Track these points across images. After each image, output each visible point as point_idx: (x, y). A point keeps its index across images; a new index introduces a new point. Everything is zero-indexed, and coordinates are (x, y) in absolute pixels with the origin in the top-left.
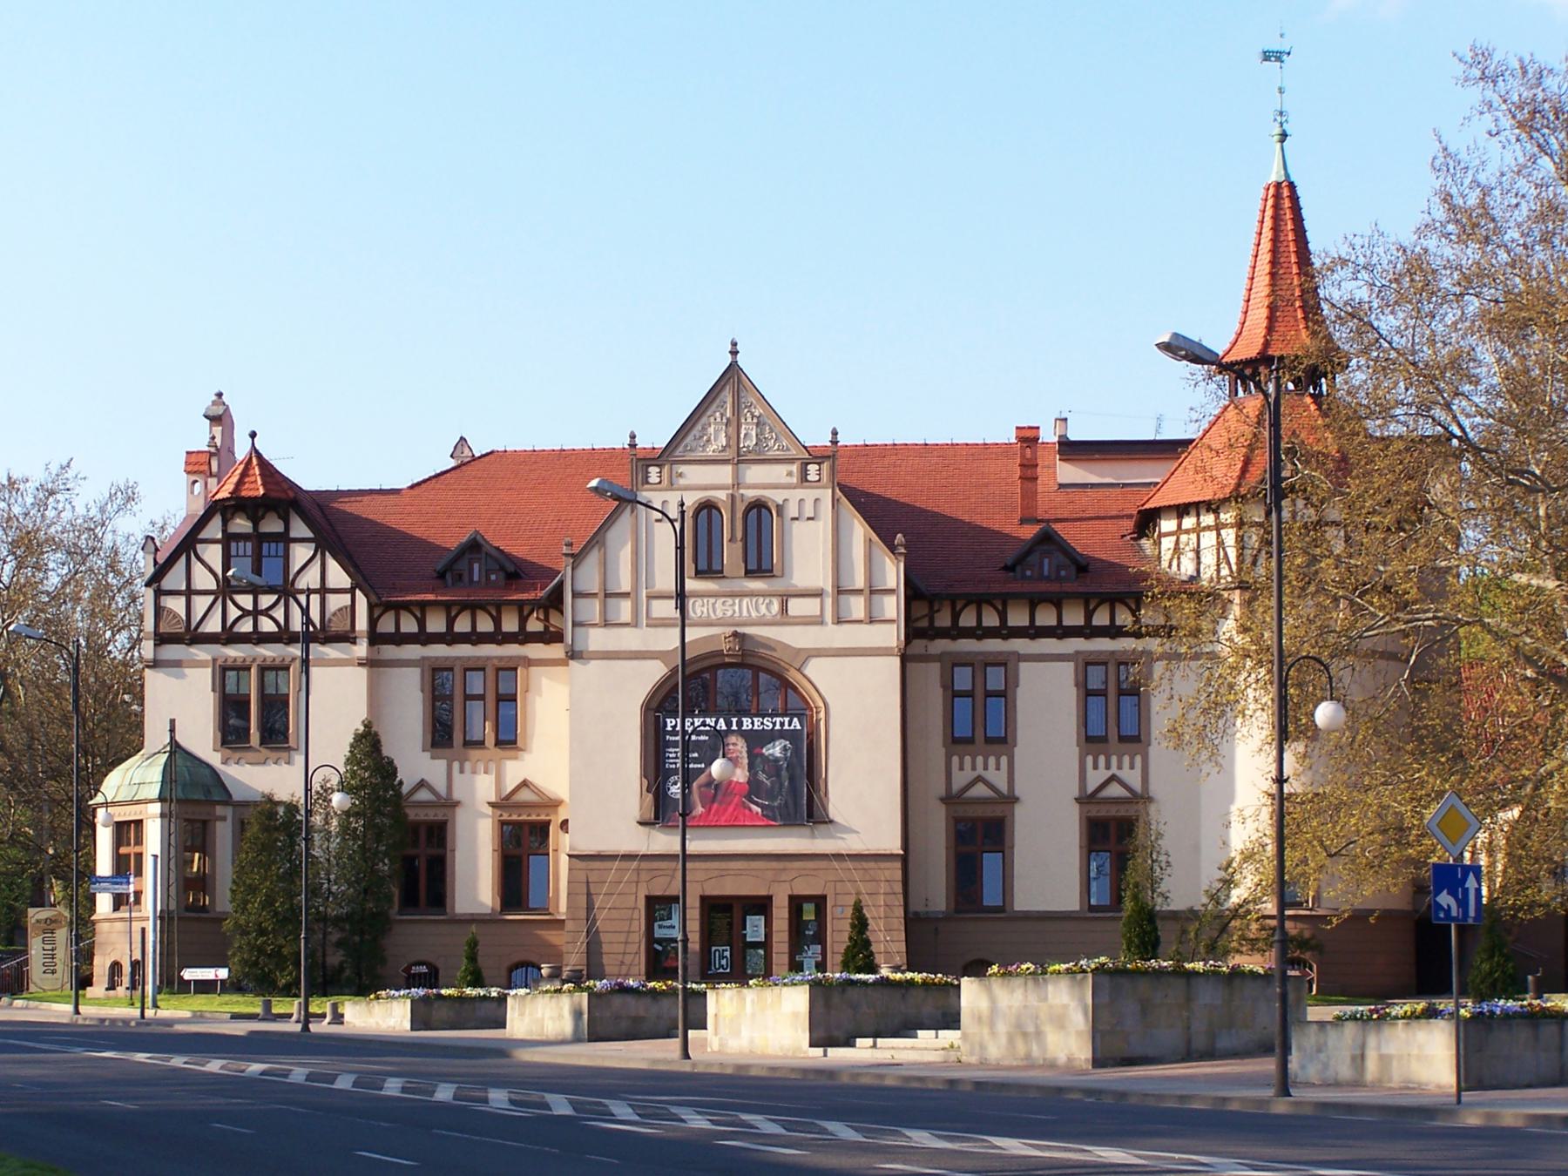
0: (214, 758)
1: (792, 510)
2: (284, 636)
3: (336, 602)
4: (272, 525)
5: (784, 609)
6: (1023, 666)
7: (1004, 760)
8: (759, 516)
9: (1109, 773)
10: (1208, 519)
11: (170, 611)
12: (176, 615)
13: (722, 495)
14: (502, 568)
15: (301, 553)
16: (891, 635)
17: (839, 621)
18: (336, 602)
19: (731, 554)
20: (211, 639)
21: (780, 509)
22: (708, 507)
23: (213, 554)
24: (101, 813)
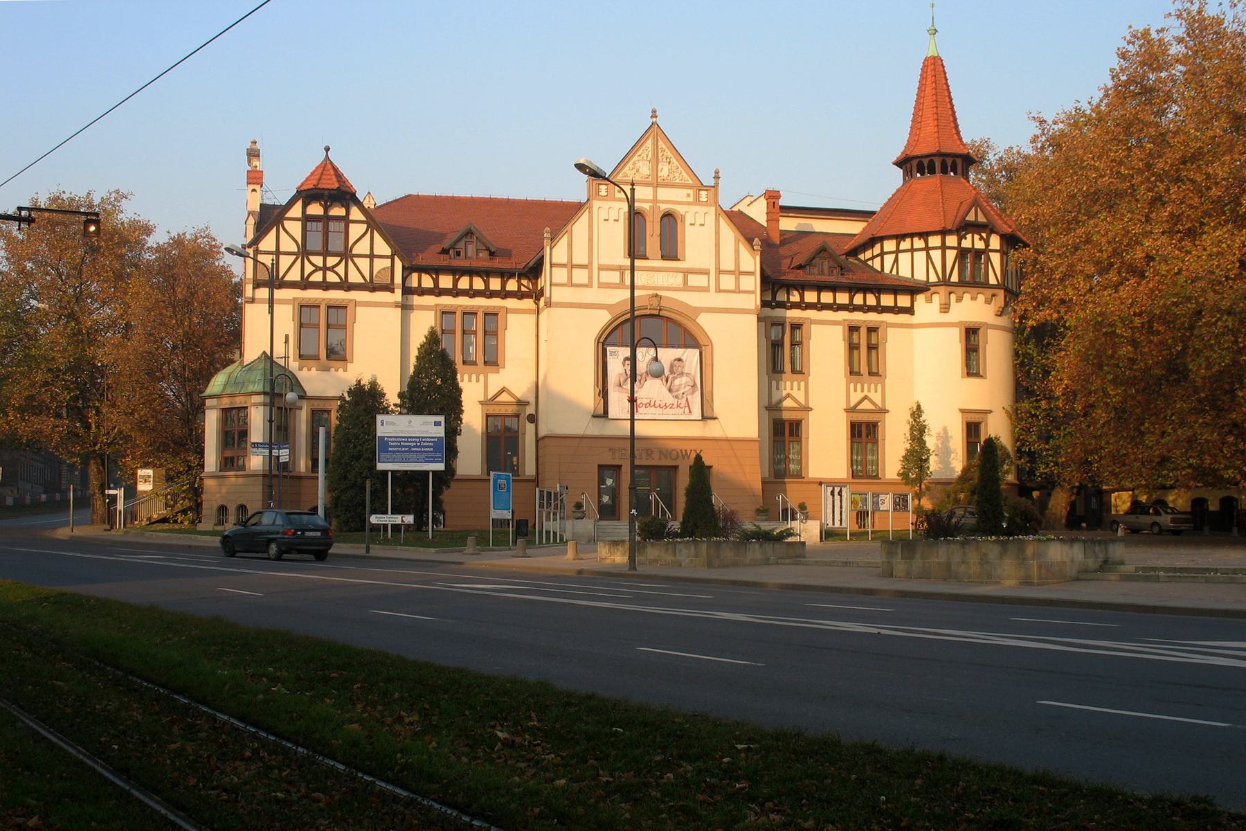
0: (293, 365)
1: (688, 221)
2: (345, 285)
3: (380, 264)
4: (338, 211)
5: (685, 281)
7: (802, 384)
8: (669, 219)
9: (863, 395)
10: (919, 243)
14: (488, 249)
15: (356, 231)
16: (754, 301)
17: (719, 290)
18: (380, 264)
19: (652, 243)
20: (293, 285)
21: (683, 217)
23: (295, 228)
24: (209, 402)
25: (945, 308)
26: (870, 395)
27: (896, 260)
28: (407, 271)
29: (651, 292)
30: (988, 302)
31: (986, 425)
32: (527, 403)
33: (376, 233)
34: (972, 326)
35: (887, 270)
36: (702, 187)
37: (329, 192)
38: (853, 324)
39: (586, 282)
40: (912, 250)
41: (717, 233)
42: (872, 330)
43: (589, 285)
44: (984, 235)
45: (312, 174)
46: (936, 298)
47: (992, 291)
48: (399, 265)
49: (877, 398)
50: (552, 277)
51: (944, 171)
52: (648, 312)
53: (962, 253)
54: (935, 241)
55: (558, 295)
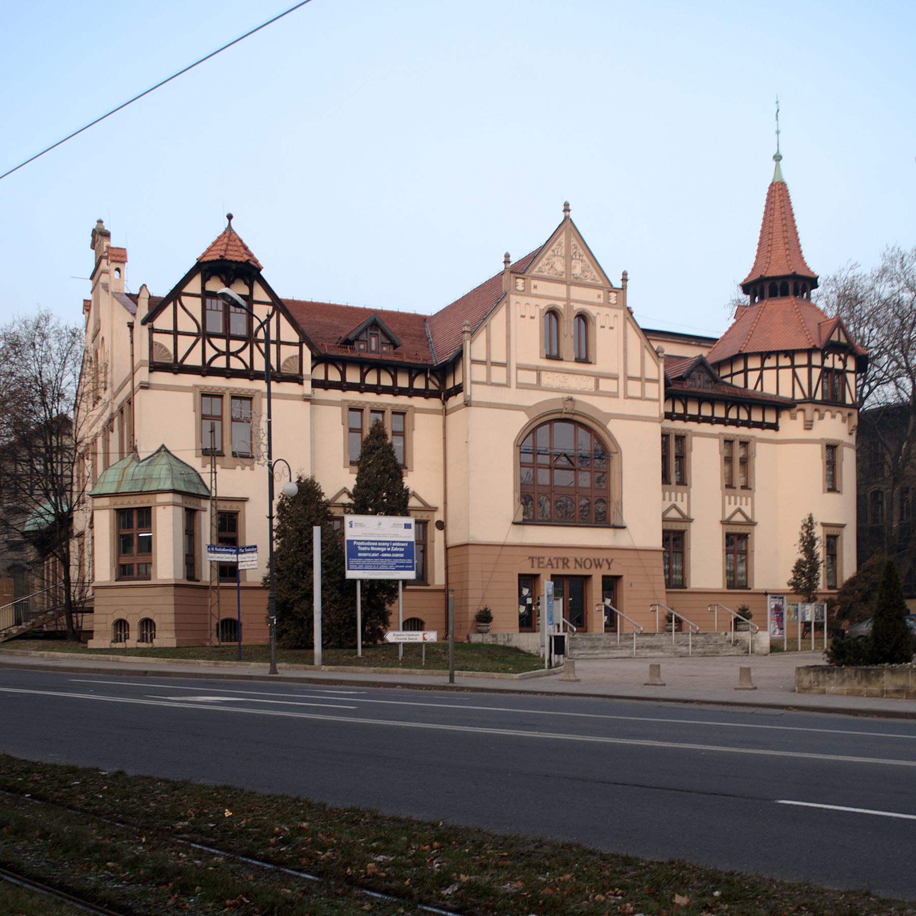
0: (196, 462)
1: (599, 322)
2: (249, 373)
3: (288, 352)
6: (695, 439)
11: (161, 346)
12: (166, 350)
13: (560, 305)
17: (627, 397)
18: (288, 352)
19: (568, 346)
20: (192, 370)
22: (553, 313)
23: (194, 305)
25: (808, 426)
26: (744, 508)
27: (761, 377)
28: (317, 360)
29: (566, 395)
30: (844, 421)
31: (842, 539)
32: (434, 510)
33: (281, 315)
34: (831, 443)
35: (751, 386)
36: (611, 289)
37: (229, 268)
38: (728, 438)
39: (504, 381)
40: (778, 368)
41: (625, 337)
42: (745, 444)
43: (507, 385)
45: (214, 244)
46: (800, 415)
47: (846, 411)
48: (307, 353)
50: (471, 373)
51: (796, 294)
52: (564, 416)
54: (801, 360)
55: (477, 393)
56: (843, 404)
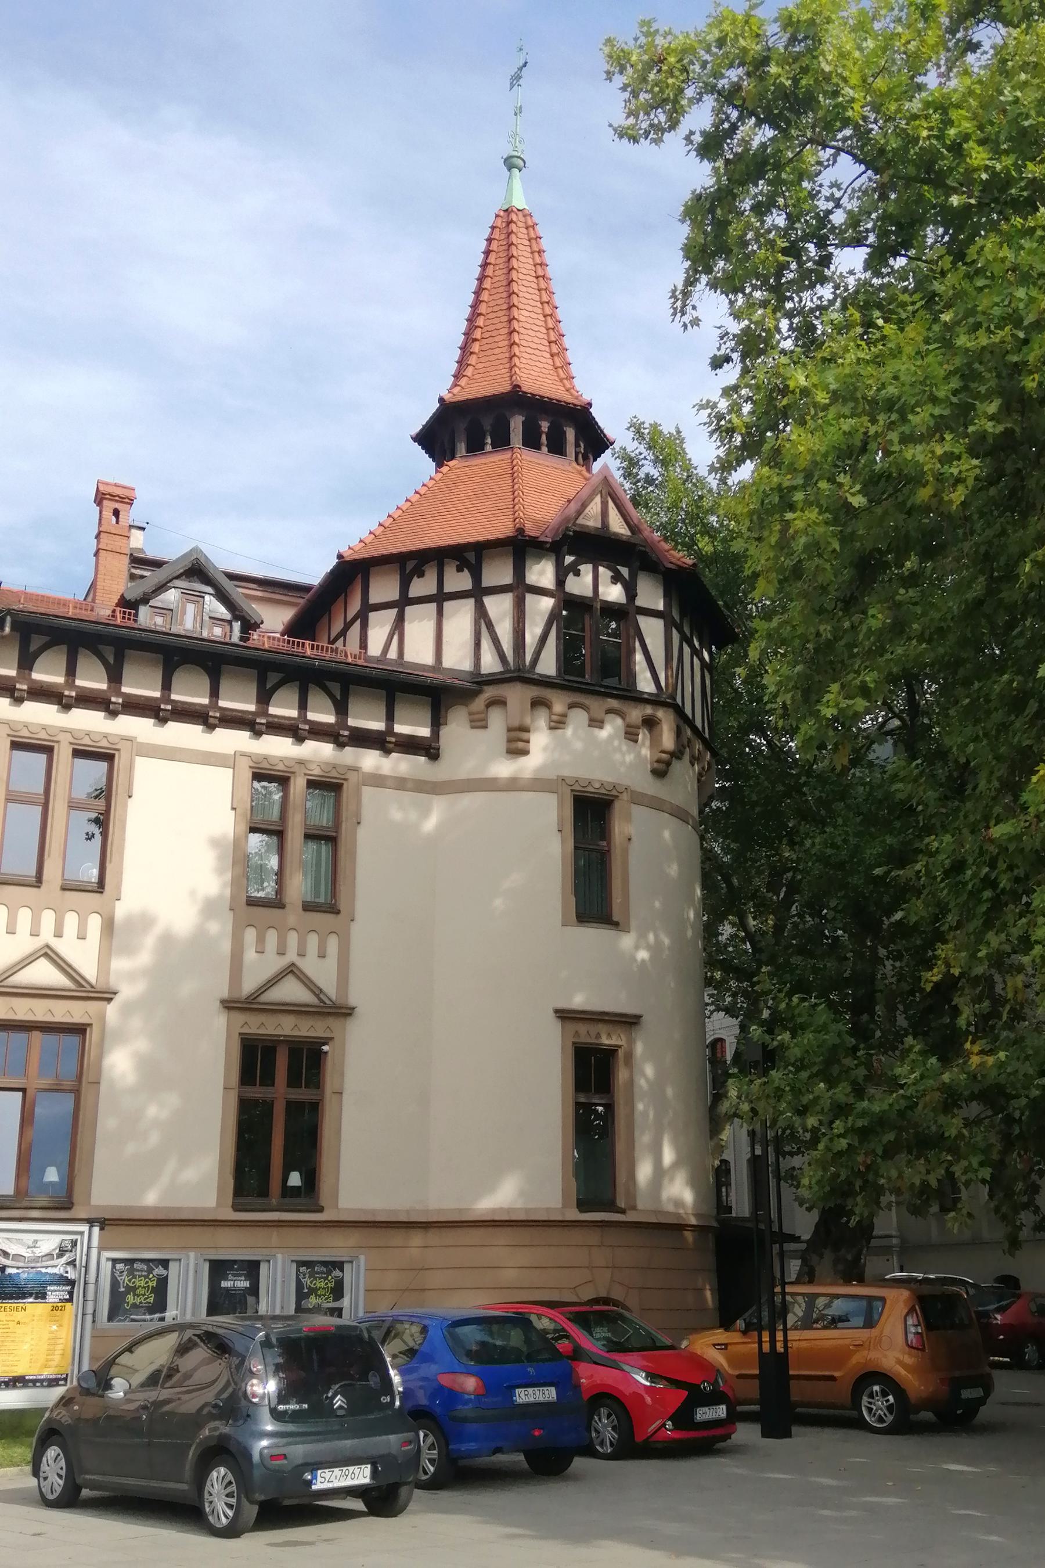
6: (143, 766)
9: (283, 962)
10: (458, 580)
26: (310, 966)
30: (631, 735)
35: (375, 648)
40: (440, 598)
44: (625, 571)
47: (636, 714)
49: (324, 973)
53: (573, 611)
56: (631, 695)
